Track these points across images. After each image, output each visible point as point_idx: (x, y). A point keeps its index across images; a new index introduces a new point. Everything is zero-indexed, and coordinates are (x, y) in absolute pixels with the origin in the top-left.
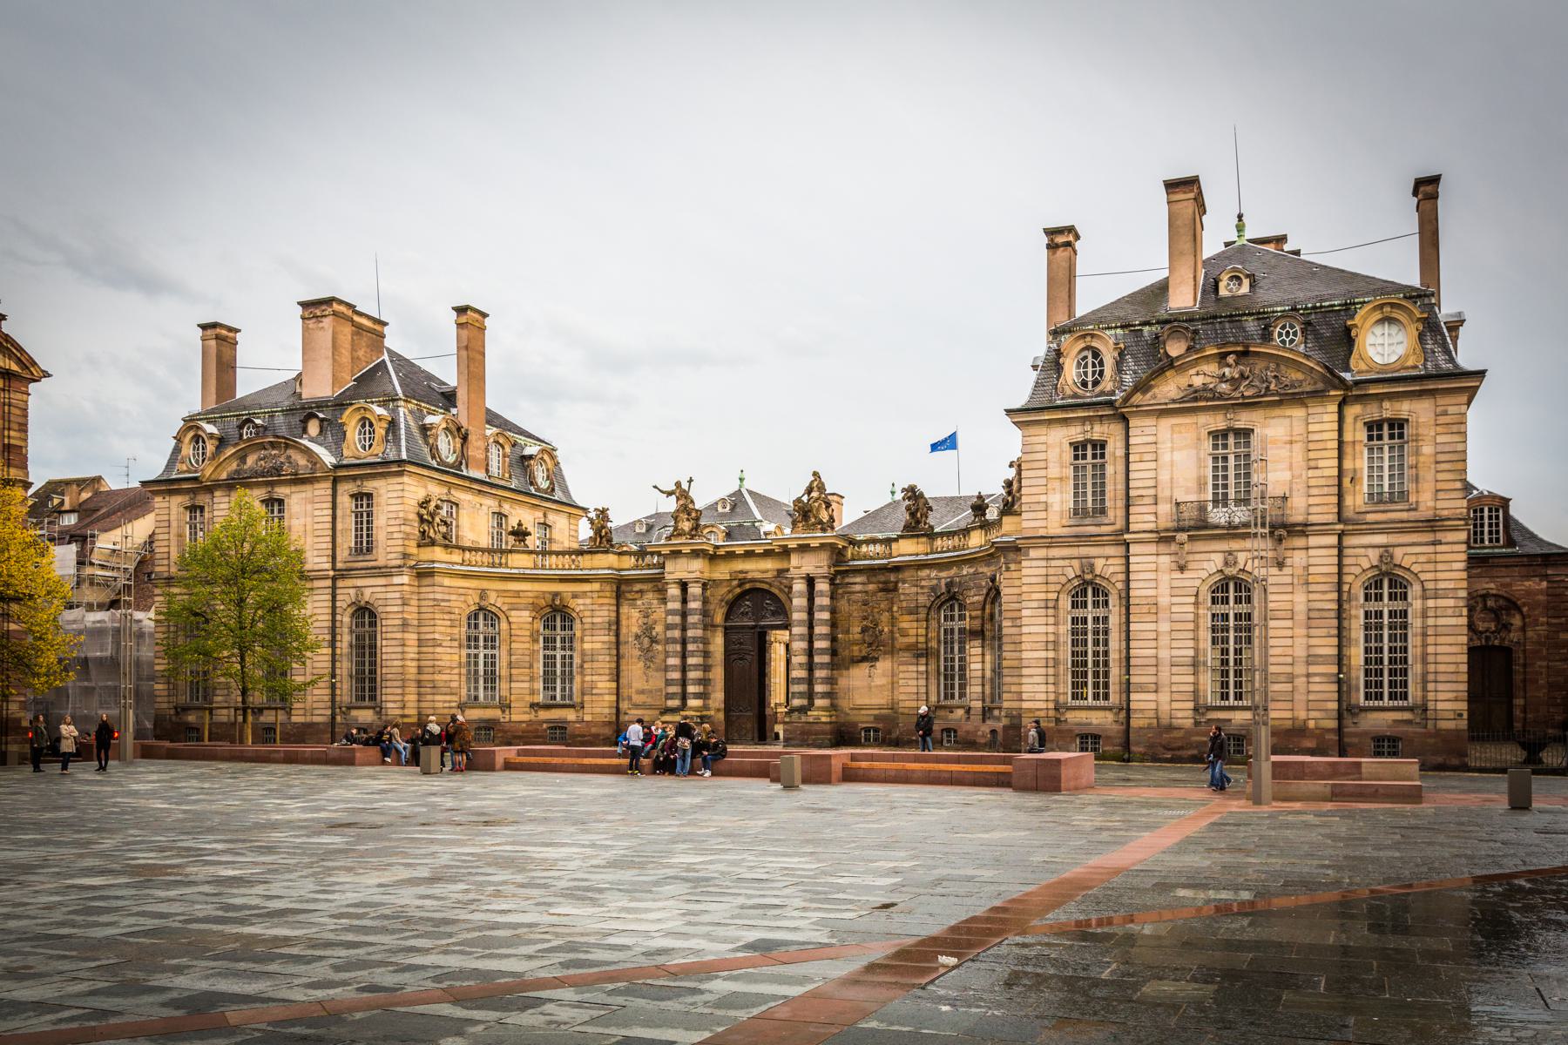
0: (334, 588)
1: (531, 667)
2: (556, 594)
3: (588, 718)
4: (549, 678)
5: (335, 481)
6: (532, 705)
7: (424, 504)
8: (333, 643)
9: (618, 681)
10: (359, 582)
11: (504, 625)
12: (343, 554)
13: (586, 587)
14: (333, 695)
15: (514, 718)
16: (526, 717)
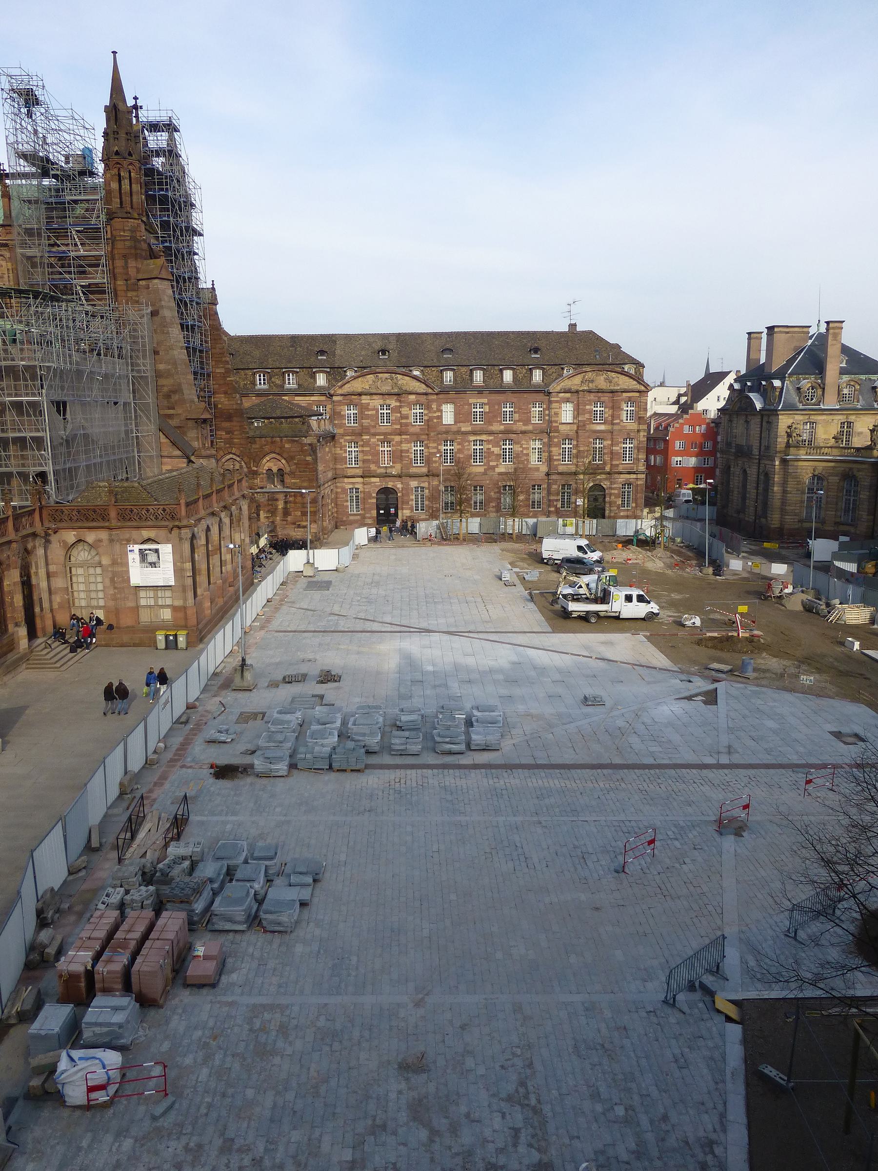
0: (759, 463)
1: (837, 504)
2: (851, 469)
3: (858, 532)
4: (847, 510)
5: (762, 416)
6: (835, 523)
7: (789, 427)
8: (757, 488)
9: (874, 515)
10: (766, 462)
11: (825, 483)
12: (763, 448)
13: (864, 466)
14: (756, 511)
15: (827, 528)
16: (832, 528)
